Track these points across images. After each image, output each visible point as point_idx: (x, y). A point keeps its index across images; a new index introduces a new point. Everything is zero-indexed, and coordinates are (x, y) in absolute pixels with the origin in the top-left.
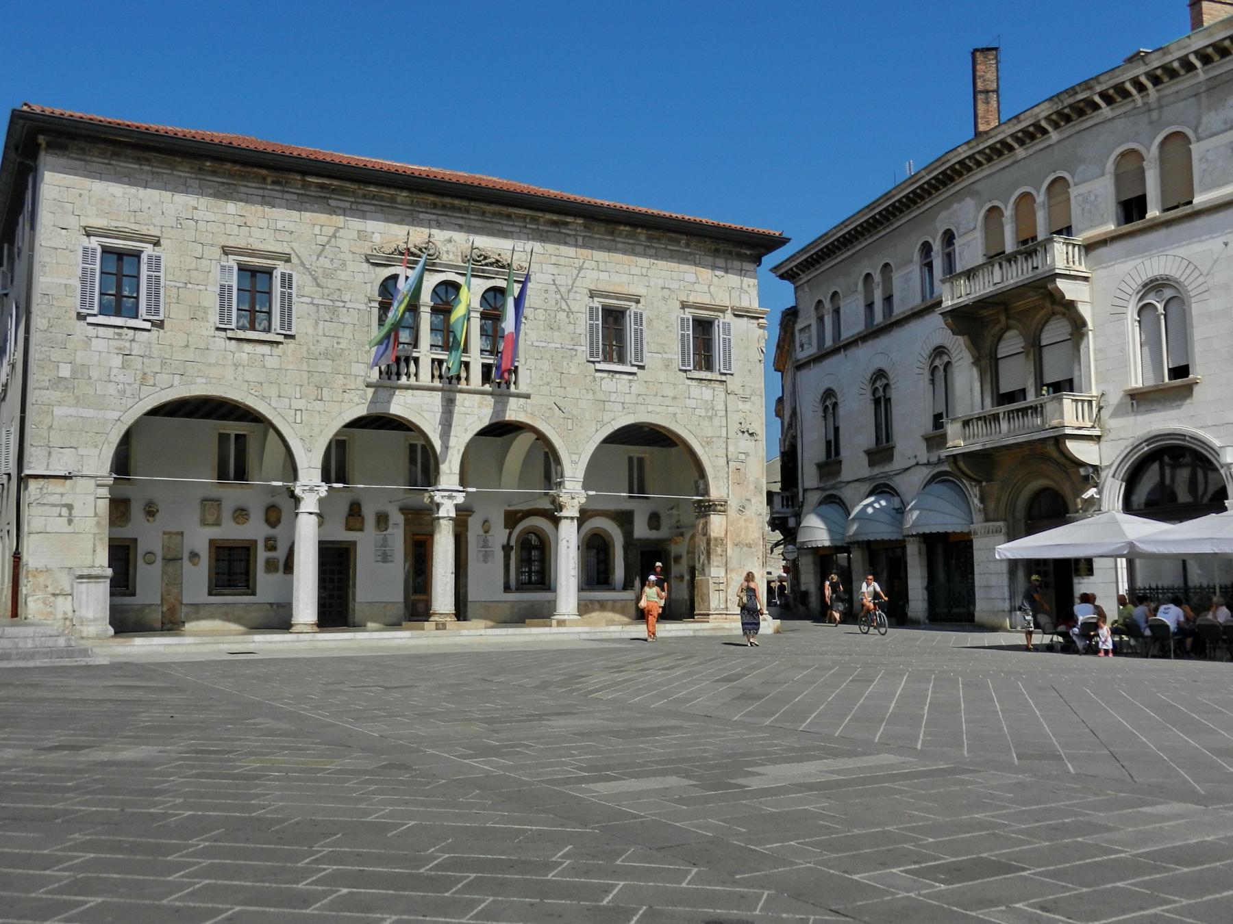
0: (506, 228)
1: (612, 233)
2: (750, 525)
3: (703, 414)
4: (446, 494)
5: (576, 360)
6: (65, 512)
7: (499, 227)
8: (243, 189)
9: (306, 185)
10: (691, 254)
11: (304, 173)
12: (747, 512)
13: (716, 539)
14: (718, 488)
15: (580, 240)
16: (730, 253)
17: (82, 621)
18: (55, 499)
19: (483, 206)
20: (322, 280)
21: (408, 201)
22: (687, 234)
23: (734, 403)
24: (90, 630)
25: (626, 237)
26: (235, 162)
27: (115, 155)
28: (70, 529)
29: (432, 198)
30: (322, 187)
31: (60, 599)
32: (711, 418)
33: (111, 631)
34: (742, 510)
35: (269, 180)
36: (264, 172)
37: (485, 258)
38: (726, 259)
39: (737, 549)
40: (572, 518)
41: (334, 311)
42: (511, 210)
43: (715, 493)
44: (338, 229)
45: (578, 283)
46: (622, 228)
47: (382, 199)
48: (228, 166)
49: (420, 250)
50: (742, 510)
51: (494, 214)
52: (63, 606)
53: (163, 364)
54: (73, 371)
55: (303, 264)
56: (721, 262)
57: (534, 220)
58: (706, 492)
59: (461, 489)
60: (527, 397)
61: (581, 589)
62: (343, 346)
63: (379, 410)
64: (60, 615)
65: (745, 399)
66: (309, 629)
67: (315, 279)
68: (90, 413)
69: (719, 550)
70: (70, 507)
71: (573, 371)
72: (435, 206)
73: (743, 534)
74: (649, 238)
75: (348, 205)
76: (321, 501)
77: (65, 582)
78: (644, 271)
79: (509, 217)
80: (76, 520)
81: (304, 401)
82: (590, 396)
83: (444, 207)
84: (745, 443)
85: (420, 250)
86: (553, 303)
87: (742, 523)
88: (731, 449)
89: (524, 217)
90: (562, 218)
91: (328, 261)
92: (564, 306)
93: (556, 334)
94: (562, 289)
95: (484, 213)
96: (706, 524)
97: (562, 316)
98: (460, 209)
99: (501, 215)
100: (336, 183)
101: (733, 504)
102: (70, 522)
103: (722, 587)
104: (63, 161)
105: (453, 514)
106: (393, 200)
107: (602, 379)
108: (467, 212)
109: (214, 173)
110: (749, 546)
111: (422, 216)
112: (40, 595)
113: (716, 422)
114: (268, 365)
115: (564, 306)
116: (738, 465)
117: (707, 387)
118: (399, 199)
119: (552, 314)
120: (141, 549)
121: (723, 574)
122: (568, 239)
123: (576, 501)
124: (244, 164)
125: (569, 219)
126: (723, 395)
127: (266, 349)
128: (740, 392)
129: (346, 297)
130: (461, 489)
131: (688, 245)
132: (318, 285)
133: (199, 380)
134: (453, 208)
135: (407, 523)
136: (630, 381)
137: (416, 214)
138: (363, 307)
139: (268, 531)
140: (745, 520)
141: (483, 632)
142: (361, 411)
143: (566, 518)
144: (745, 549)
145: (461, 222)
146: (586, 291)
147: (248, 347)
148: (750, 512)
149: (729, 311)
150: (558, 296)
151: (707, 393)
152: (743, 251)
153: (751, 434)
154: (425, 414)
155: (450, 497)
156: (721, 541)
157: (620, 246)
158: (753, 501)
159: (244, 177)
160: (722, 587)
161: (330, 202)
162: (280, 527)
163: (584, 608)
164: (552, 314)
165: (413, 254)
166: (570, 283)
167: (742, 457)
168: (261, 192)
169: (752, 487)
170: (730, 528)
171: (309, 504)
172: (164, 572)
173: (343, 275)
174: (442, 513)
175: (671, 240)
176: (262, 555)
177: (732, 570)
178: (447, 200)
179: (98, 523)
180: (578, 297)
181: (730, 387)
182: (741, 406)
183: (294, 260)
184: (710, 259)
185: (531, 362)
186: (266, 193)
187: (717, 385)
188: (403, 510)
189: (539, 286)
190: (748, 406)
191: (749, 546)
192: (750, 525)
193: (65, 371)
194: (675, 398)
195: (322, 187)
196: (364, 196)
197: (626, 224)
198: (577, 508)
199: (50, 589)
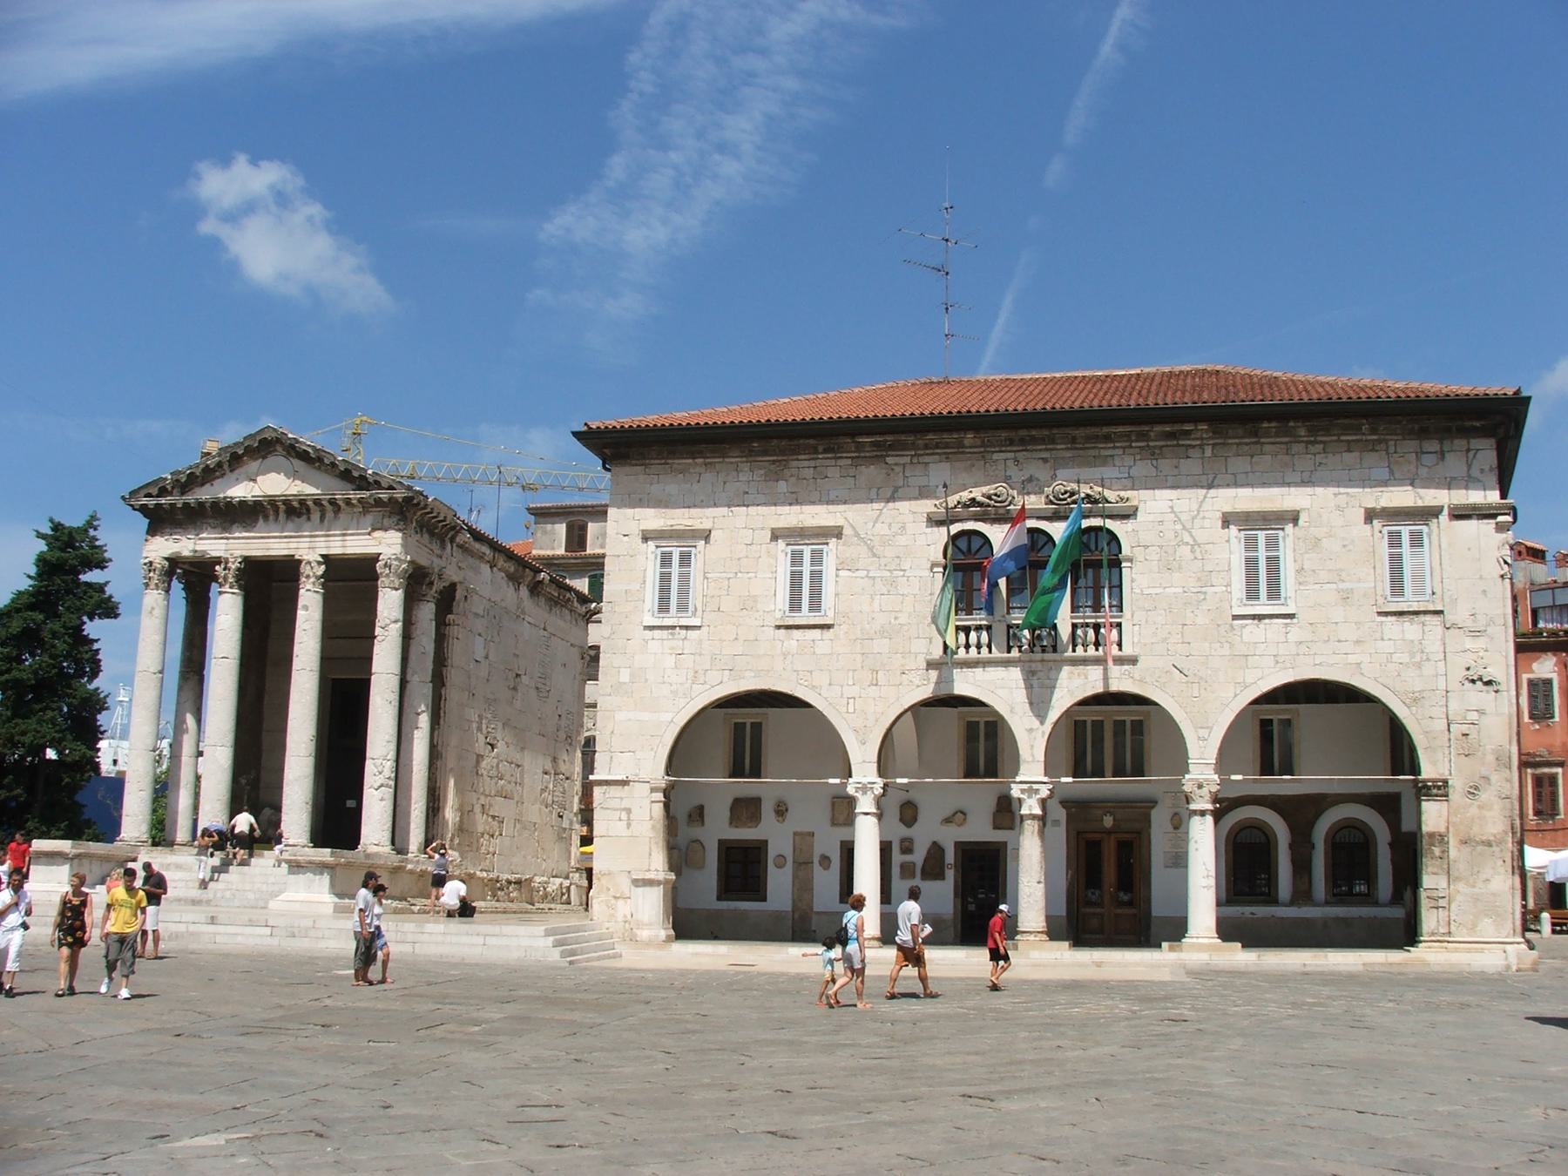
0: (1104, 453)
1: (1256, 435)
2: (1488, 814)
3: (1405, 658)
4: (1025, 786)
5: (1205, 607)
6: (624, 816)
7: (1096, 452)
8: (795, 463)
9: (860, 447)
10: (1379, 442)
11: (853, 435)
12: (1484, 796)
13: (1431, 835)
14: (1434, 763)
15: (1208, 452)
16: (1448, 430)
17: (640, 925)
18: (615, 803)
19: (1068, 431)
20: (878, 550)
21: (979, 442)
22: (1365, 416)
23: (1458, 640)
24: (644, 934)
25: (1277, 436)
26: (780, 437)
27: (673, 454)
28: (626, 833)
29: (1004, 434)
30: (875, 444)
31: (621, 902)
32: (1419, 666)
33: (663, 932)
34: (1473, 791)
35: (820, 449)
36: (812, 442)
37: (1072, 494)
38: (1441, 440)
39: (1466, 849)
40: (1203, 813)
41: (893, 583)
42: (1106, 430)
43: (1429, 770)
44: (896, 489)
45: (1206, 506)
46: (1265, 425)
47: (947, 446)
48: (775, 442)
49: (989, 498)
50: (1473, 791)
51: (1089, 439)
52: (623, 909)
53: (713, 659)
54: (632, 675)
55: (857, 535)
56: (1433, 445)
57: (1143, 436)
58: (1415, 769)
59: (1046, 779)
60: (1133, 661)
61: (1218, 904)
62: (903, 619)
63: (943, 692)
64: (620, 918)
65: (1476, 633)
66: (876, 943)
67: (871, 549)
68: (646, 716)
69: (1437, 851)
70: (629, 811)
71: (1199, 621)
72: (1012, 443)
74: (1312, 431)
75: (908, 459)
76: (879, 801)
77: (625, 884)
78: (1306, 475)
79: (1107, 438)
80: (634, 824)
81: (856, 688)
82: (1226, 651)
83: (1022, 441)
84: (1479, 697)
85: (989, 498)
86: (1172, 535)
87: (1474, 811)
88: (1453, 706)
89: (1127, 436)
90: (1177, 427)
91: (885, 526)
92: (1187, 538)
93: (1176, 575)
94: (1183, 517)
95: (1074, 440)
96: (1419, 813)
97: (1185, 551)
98: (1042, 441)
99: (1096, 438)
100: (889, 438)
101: (1457, 785)
102: (629, 825)
103: (1442, 903)
104: (627, 469)
105: (1038, 811)
106: (960, 445)
107: (1244, 627)
108: (1053, 442)
109: (765, 453)
110: (1489, 844)
111: (995, 456)
112: (603, 897)
113: (1428, 669)
114: (818, 651)
115: (1187, 538)
116: (1465, 729)
117: (1411, 622)
118: (966, 442)
119: (1171, 551)
120: (772, 853)
121: (1445, 885)
122: (1191, 452)
123: (1205, 791)
124: (791, 437)
125: (1187, 427)
126: (1440, 629)
127: (818, 631)
128: (1469, 623)
129: (906, 566)
130: (1046, 779)
131: (1374, 431)
132: (874, 555)
133: (748, 674)
134: (1034, 440)
135: (1070, 819)
137: (988, 456)
138: (927, 573)
139: (904, 831)
140: (1480, 807)
141: (1058, 955)
142: (926, 692)
143: (1195, 812)
144: (1480, 848)
145: (1044, 455)
146: (1219, 515)
147: (796, 633)
149: (1446, 512)
150: (1179, 527)
151: (1410, 629)
152: (1468, 424)
153: (1489, 683)
154: (1000, 692)
156: (1441, 839)
157: (1267, 448)
158: (1494, 778)
159: (795, 451)
160: (1442, 903)
161: (888, 460)
162: (916, 826)
163: (1228, 931)
164: (1171, 551)
165: (980, 504)
166: (1195, 506)
167: (1473, 716)
168: (812, 463)
169: (1490, 758)
170: (1453, 819)
171: (866, 804)
172: (795, 877)
173: (902, 540)
174: (1024, 811)
175: (1347, 429)
177: (1458, 879)
178: (1023, 433)
179: (653, 827)
180: (1207, 523)
181: (1450, 617)
182: (1469, 643)
183: (847, 531)
184: (1412, 445)
185: (1139, 616)
186: (818, 463)
187: (1428, 618)
188: (1065, 803)
189: (1151, 518)
190: (1481, 643)
191: (1489, 844)
193: (625, 676)
194: (1358, 642)
195: (875, 444)
196: (926, 447)
197: (1269, 420)
198: (1208, 797)
199: (612, 892)
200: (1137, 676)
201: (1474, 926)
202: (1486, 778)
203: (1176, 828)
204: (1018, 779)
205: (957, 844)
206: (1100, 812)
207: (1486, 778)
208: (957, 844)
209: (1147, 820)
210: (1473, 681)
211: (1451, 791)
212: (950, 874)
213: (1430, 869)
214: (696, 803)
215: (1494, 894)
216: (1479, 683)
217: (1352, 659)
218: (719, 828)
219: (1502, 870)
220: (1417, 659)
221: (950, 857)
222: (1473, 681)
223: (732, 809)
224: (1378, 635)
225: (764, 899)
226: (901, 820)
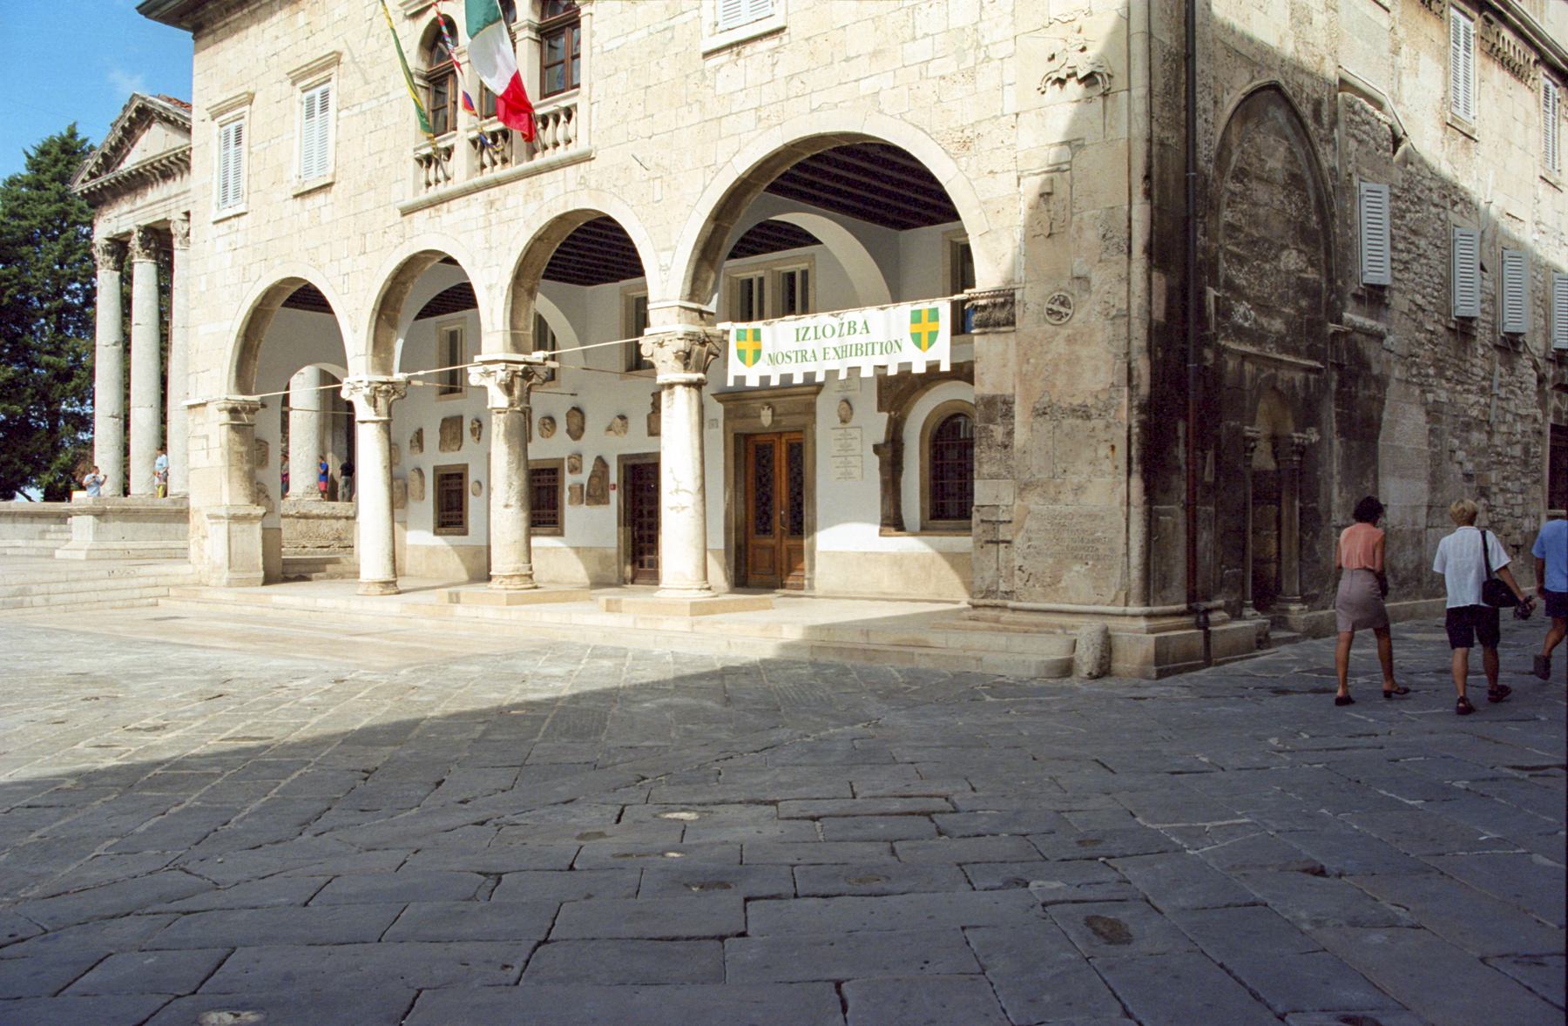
2: (1084, 352)
3: (950, 67)
32: (971, 75)
34: (1059, 309)
39: (1045, 425)
50: (1059, 309)
69: (998, 432)
73: (1061, 381)
87: (1059, 347)
107: (718, 69)
136: (775, 50)
140: (1070, 340)
143: (663, 386)
144: (1069, 422)
148: (1087, 312)
155: (488, 374)
158: (1096, 278)
169: (1091, 236)
176: (569, 479)
191: (1084, 413)
192: (1084, 352)
194: (875, 54)
200: (593, 184)
201: (1056, 579)
202: (1083, 280)
203: (844, 421)
204: (477, 358)
205: (621, 458)
206: (758, 405)
207: (1083, 280)
208: (621, 458)
209: (810, 409)
210: (1061, 82)
211: (1018, 311)
212: (614, 496)
213: (986, 469)
214: (416, 429)
215: (1092, 516)
216: (1072, 83)
217: (866, 87)
218: (434, 457)
219: (1107, 466)
220: (970, 62)
221: (614, 477)
222: (1061, 82)
223: (442, 431)
224: (908, 32)
225: (465, 533)
226: (568, 431)
